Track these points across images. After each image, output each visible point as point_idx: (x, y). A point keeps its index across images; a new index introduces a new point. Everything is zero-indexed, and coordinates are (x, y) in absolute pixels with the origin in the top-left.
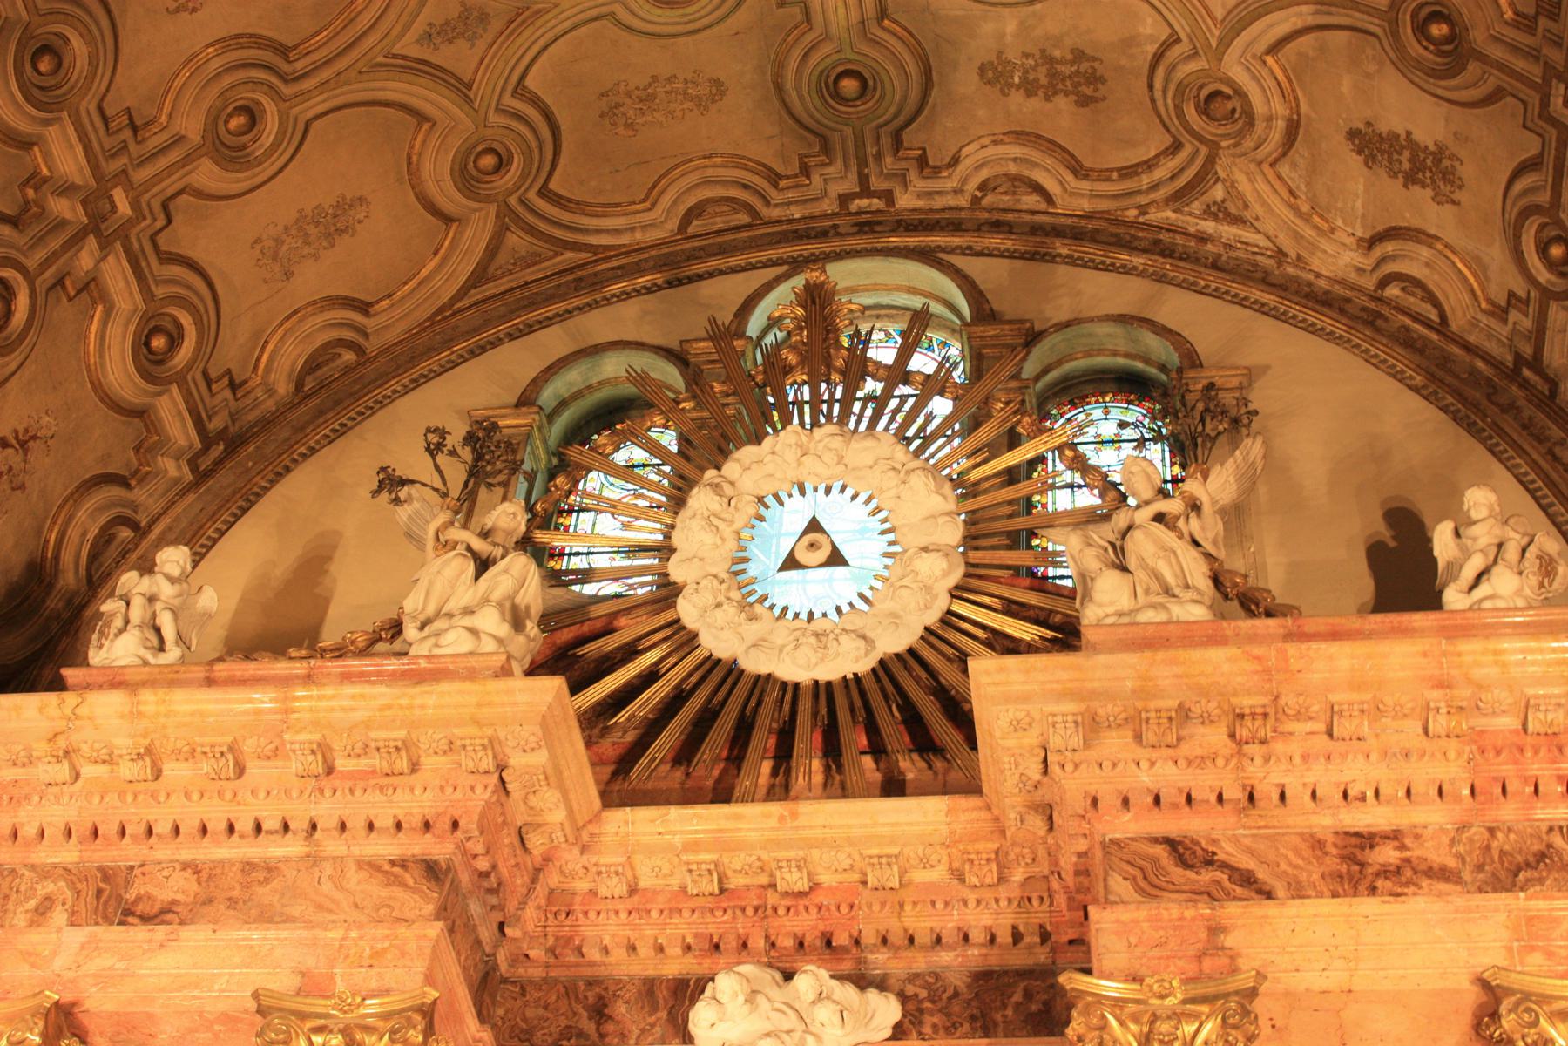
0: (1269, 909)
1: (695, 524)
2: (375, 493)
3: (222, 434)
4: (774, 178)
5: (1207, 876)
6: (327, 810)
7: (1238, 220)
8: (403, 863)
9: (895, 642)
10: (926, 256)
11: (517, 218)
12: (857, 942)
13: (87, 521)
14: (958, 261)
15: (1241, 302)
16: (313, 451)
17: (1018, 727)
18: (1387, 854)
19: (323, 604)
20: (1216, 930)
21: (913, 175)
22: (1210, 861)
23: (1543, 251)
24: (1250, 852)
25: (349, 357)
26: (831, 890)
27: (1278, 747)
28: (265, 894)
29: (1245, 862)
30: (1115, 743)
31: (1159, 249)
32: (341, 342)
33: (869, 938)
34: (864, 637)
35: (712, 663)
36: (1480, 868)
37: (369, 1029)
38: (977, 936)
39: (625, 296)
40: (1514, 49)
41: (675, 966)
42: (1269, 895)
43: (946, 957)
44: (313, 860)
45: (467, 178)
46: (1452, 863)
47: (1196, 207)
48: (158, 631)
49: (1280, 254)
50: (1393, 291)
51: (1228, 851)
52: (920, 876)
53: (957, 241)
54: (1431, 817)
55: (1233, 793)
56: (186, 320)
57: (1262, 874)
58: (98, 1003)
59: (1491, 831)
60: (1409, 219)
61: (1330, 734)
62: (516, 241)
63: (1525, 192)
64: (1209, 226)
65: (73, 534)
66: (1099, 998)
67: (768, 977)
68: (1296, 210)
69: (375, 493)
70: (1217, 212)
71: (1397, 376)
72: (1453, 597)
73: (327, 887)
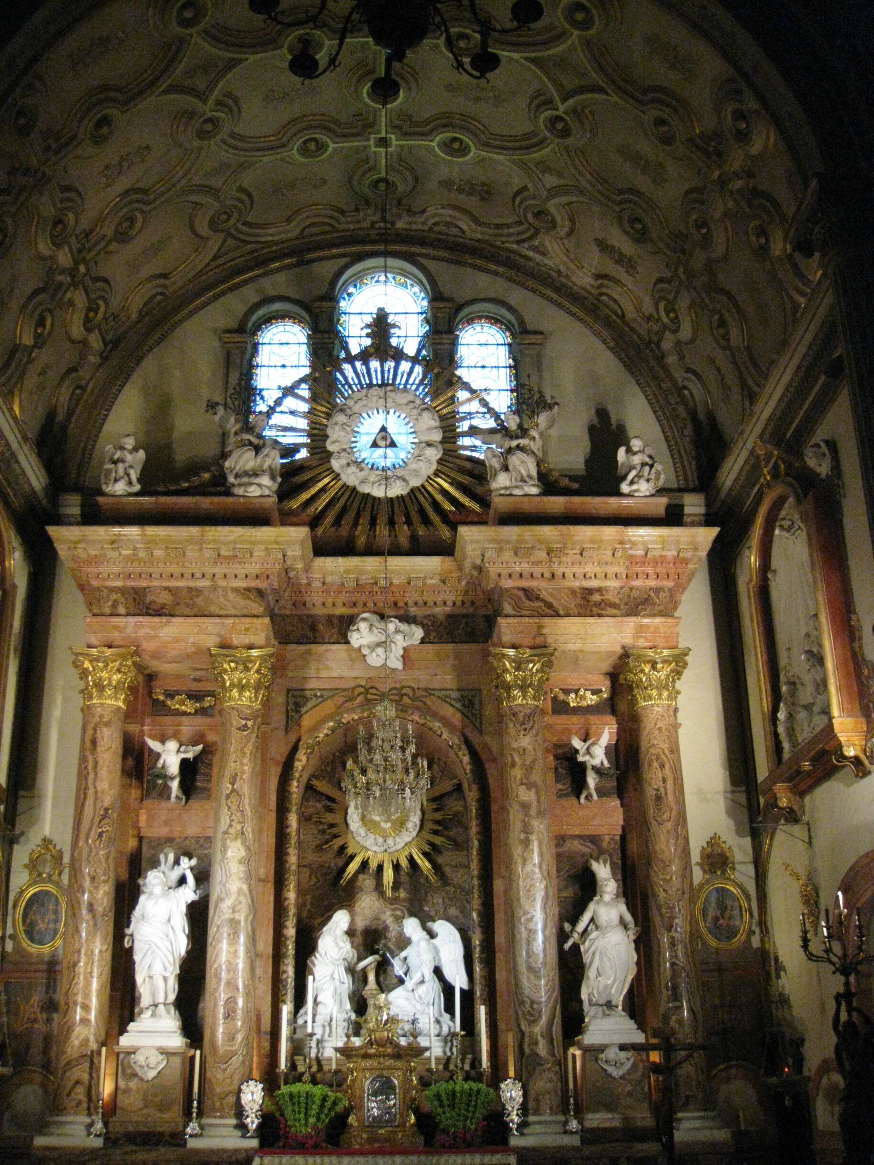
0: (559, 621)
1: (337, 428)
2: (207, 411)
3: (111, 342)
4: (342, 212)
5: (537, 604)
6: (219, 570)
7: (543, 254)
8: (248, 590)
9: (415, 482)
10: (410, 258)
11: (232, 236)
12: (406, 604)
13: (64, 395)
14: (425, 262)
15: (543, 296)
16: (151, 349)
17: (475, 549)
18: (597, 597)
19: (170, 429)
20: (540, 627)
21: (404, 214)
22: (538, 598)
23: (667, 315)
24: (551, 594)
25: (159, 298)
26: (398, 586)
27: (564, 559)
28: (199, 601)
29: (550, 600)
30: (508, 555)
31: (509, 263)
32: (158, 294)
33: (411, 603)
34: (404, 480)
35: (345, 486)
36: (626, 604)
37: (251, 662)
38: (450, 603)
39: (279, 270)
40: (668, 245)
41: (340, 611)
42: (558, 615)
43: (438, 610)
44: (214, 588)
45: (213, 225)
46: (617, 601)
47: (526, 245)
48: (128, 475)
49: (559, 272)
50: (604, 298)
51: (544, 595)
52: (429, 582)
53: (424, 251)
54: (612, 584)
55: (547, 575)
56: (101, 303)
57: (555, 604)
58: (148, 646)
59: (631, 589)
60: (613, 274)
61: (581, 554)
62: (230, 241)
63: (662, 290)
64: (531, 254)
65: (61, 399)
66: (504, 656)
67: (374, 618)
68: (568, 257)
69: (207, 411)
70: (536, 249)
71: (604, 342)
72: (625, 488)
73: (221, 599)
